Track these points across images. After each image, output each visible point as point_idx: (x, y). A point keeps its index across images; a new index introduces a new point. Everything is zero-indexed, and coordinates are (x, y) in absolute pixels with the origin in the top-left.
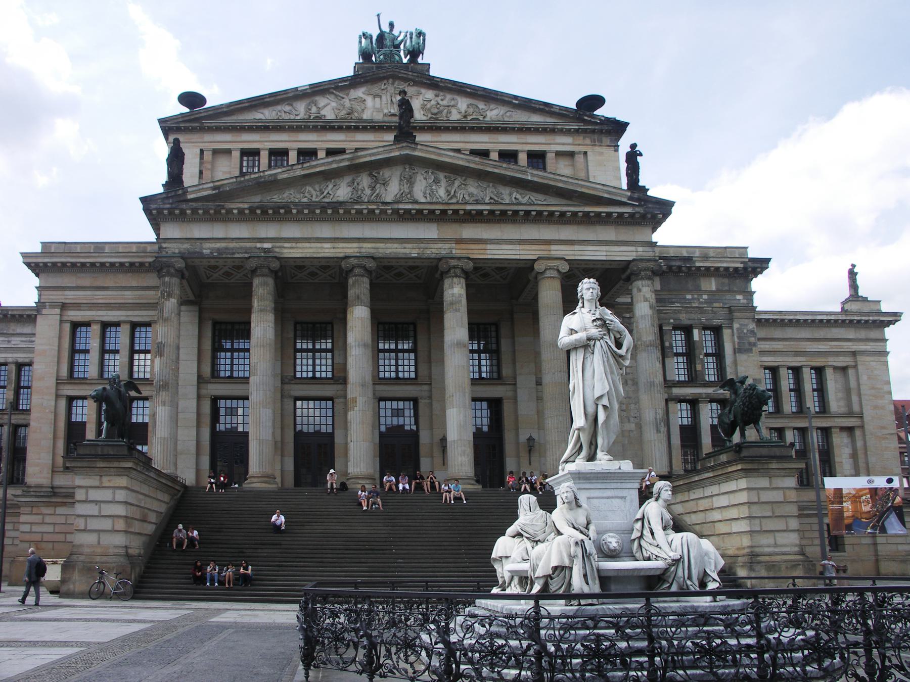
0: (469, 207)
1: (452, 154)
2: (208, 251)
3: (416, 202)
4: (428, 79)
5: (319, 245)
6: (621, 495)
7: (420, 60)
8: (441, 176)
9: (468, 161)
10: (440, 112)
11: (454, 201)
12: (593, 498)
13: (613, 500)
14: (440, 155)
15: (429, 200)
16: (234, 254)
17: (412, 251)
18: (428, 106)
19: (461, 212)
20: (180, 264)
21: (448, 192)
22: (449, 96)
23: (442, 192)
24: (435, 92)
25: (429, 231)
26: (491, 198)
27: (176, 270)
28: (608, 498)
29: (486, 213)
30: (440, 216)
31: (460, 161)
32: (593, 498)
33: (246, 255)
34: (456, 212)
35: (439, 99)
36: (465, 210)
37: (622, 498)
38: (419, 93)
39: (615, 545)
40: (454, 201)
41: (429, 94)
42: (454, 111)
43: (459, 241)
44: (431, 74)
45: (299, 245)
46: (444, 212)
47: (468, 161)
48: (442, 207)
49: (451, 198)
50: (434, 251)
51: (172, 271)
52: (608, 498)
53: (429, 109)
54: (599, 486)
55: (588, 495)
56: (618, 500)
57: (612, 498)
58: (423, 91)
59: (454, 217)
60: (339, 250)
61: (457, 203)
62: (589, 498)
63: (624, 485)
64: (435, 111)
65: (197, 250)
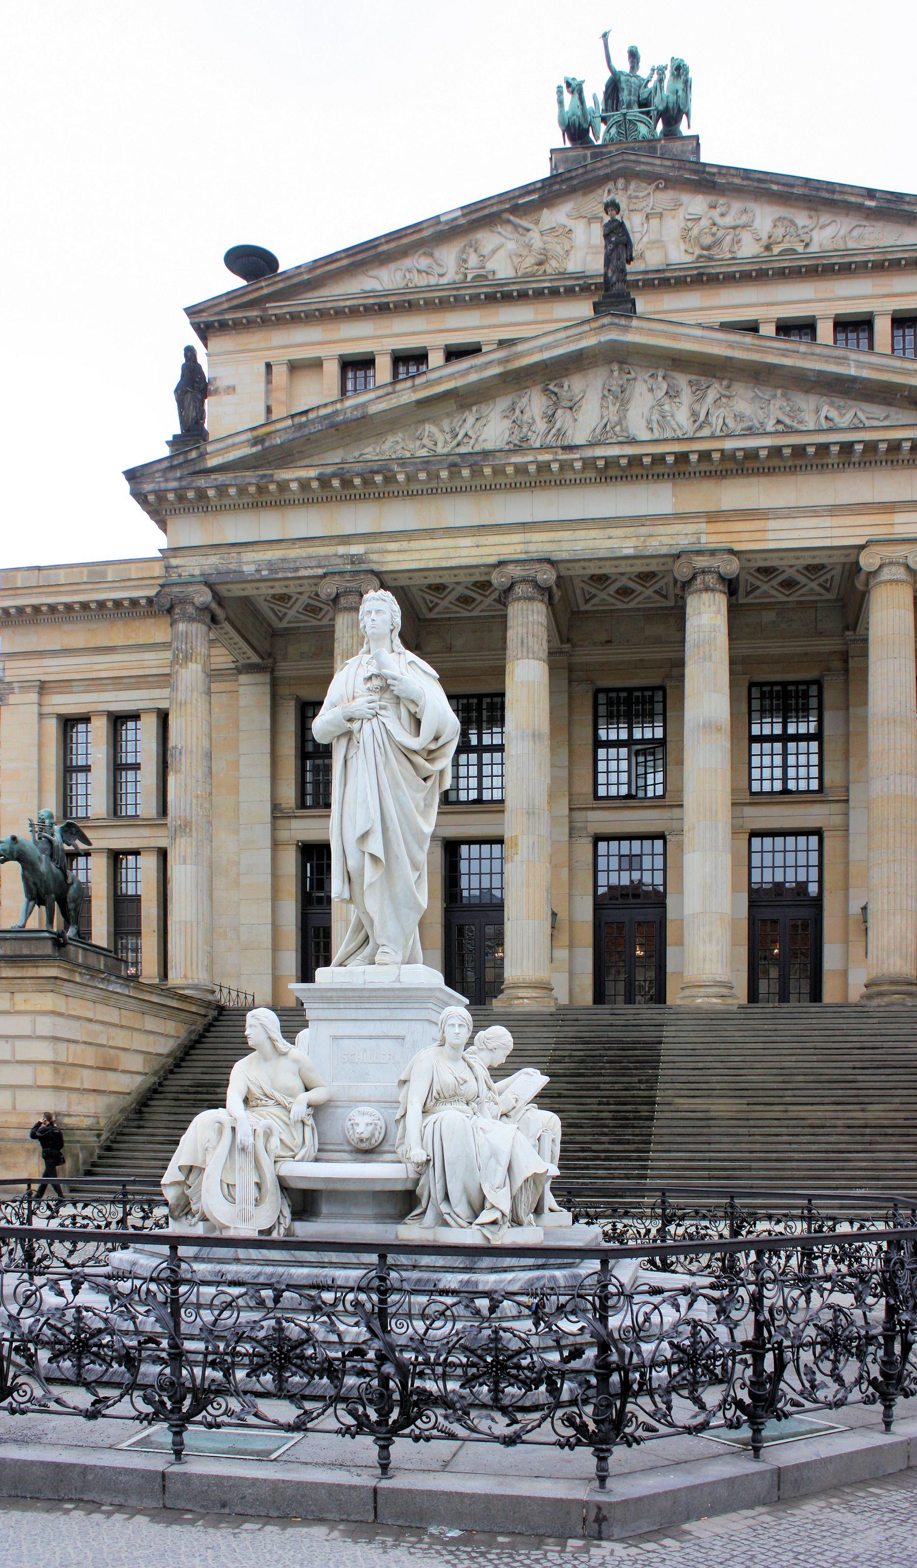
0: (729, 445)
1: (699, 332)
2: (253, 568)
3: (633, 441)
4: (695, 172)
5: (450, 542)
6: (395, 1032)
7: (684, 128)
8: (682, 380)
9: (731, 345)
10: (717, 243)
11: (706, 432)
12: (342, 1038)
13: (381, 1042)
14: (675, 337)
15: (656, 435)
16: (297, 569)
17: (623, 543)
18: (695, 232)
19: (716, 456)
20: (204, 597)
21: (694, 414)
22: (737, 206)
23: (681, 417)
24: (710, 199)
25: (657, 499)
26: (779, 422)
27: (197, 608)
28: (371, 1038)
29: (763, 453)
30: (676, 467)
31: (719, 346)
32: (342, 1038)
33: (320, 572)
34: (705, 456)
35: (715, 214)
36: (722, 451)
37: (397, 1038)
38: (678, 205)
39: (359, 1129)
40: (706, 432)
41: (696, 204)
42: (746, 237)
43: (713, 517)
44: (704, 159)
45: (415, 545)
46: (682, 458)
47: (731, 345)
48: (677, 448)
49: (701, 427)
50: (665, 540)
51: (190, 610)
52: (371, 1038)
53: (697, 238)
54: (353, 1014)
55: (334, 1032)
56: (390, 1043)
57: (379, 1038)
58: (685, 198)
59: (704, 467)
60: (482, 551)
61: (713, 437)
62: (335, 1038)
63: (399, 1014)
64: (707, 240)
65: (233, 567)
